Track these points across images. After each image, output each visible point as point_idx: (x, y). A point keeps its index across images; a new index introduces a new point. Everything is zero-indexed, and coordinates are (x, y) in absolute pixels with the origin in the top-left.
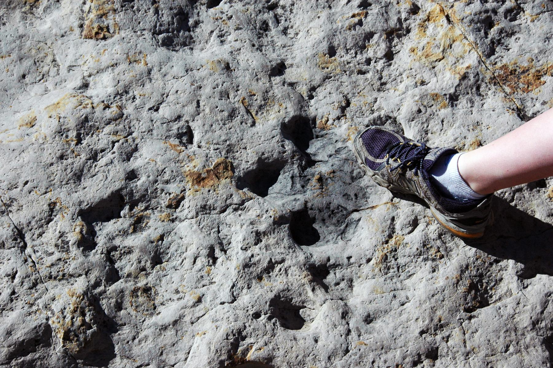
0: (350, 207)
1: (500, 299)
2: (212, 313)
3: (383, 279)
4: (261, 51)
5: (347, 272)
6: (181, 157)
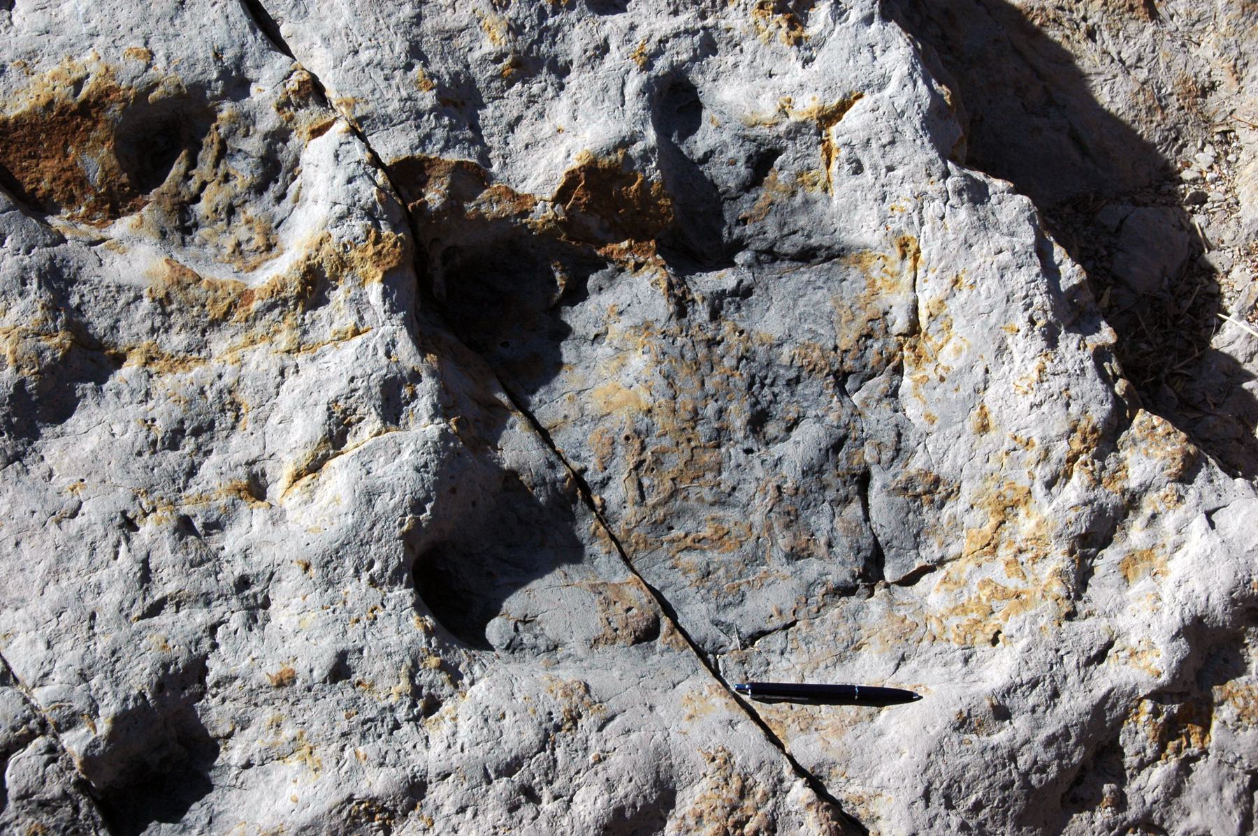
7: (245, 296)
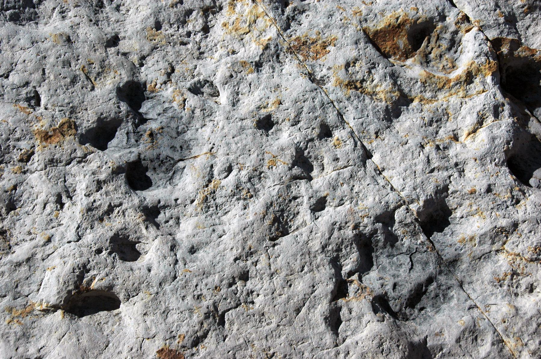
0: (176, 158)
1: (297, 229)
2: (60, 250)
3: (204, 216)
4: (98, 25)
5: (175, 212)
6: (30, 118)
7: (449, 81)
